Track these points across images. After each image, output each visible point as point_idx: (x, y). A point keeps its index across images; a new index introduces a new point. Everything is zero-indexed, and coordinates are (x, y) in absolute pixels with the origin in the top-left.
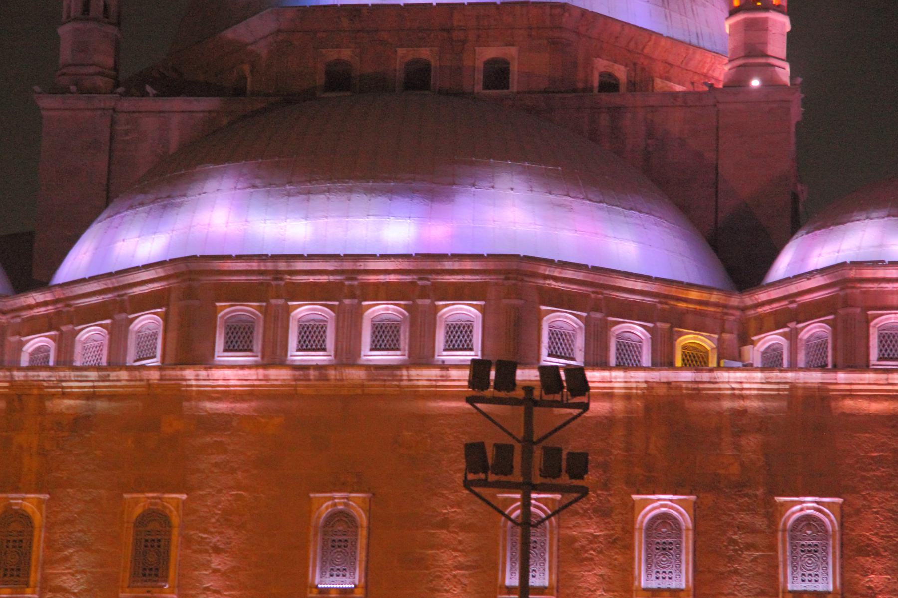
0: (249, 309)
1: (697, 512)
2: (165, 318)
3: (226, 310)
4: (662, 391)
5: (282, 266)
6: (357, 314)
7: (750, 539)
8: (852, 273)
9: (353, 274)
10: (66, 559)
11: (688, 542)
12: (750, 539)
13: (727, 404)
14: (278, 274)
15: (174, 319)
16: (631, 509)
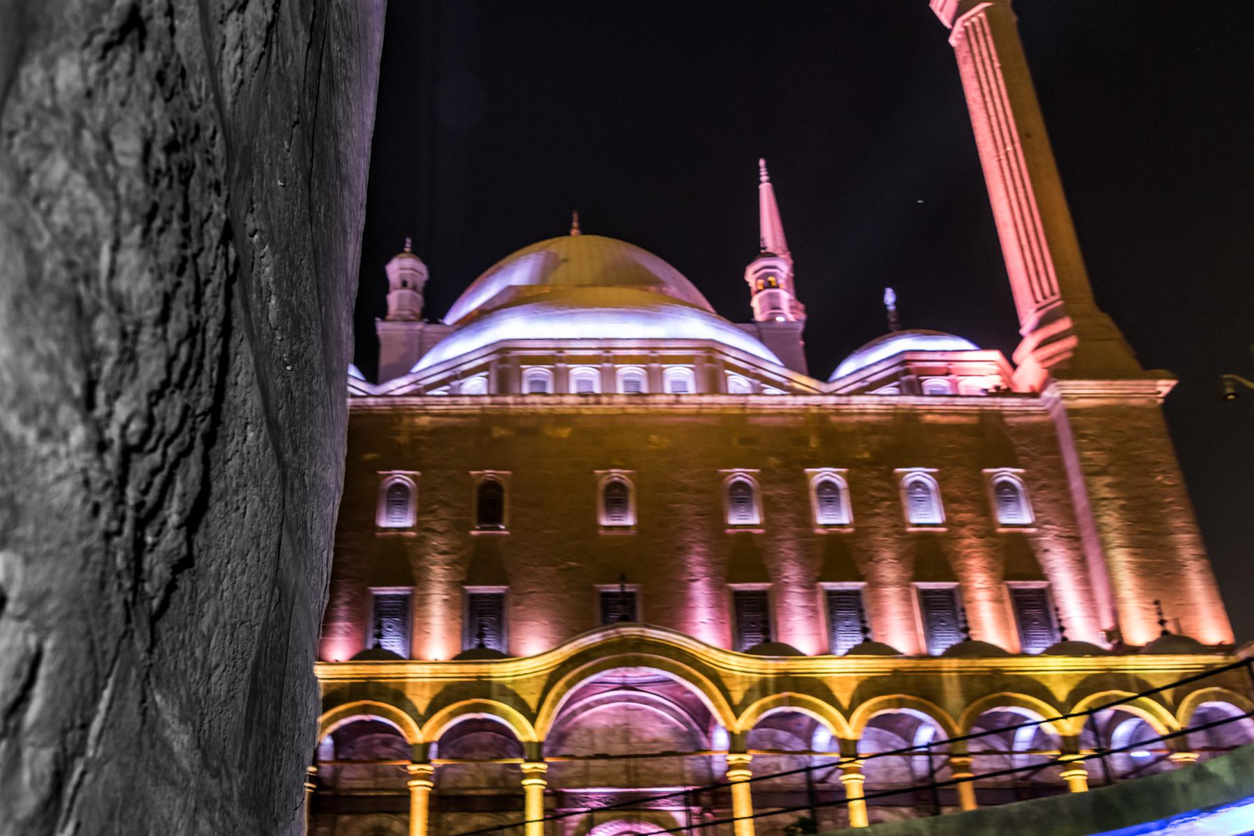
0: (543, 371)
1: (848, 477)
2: (487, 377)
3: (530, 371)
4: (814, 410)
5: (563, 345)
6: (613, 372)
7: (883, 495)
8: (908, 357)
9: (607, 349)
10: (433, 511)
11: (845, 499)
12: (883, 495)
13: (856, 418)
14: (560, 350)
15: (493, 378)
16: (805, 479)
